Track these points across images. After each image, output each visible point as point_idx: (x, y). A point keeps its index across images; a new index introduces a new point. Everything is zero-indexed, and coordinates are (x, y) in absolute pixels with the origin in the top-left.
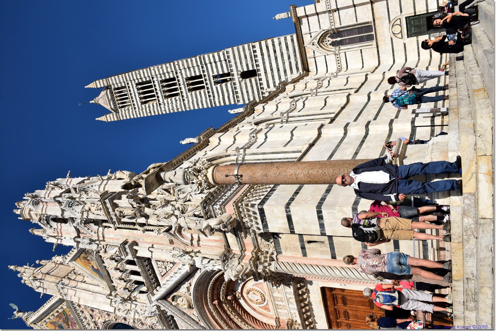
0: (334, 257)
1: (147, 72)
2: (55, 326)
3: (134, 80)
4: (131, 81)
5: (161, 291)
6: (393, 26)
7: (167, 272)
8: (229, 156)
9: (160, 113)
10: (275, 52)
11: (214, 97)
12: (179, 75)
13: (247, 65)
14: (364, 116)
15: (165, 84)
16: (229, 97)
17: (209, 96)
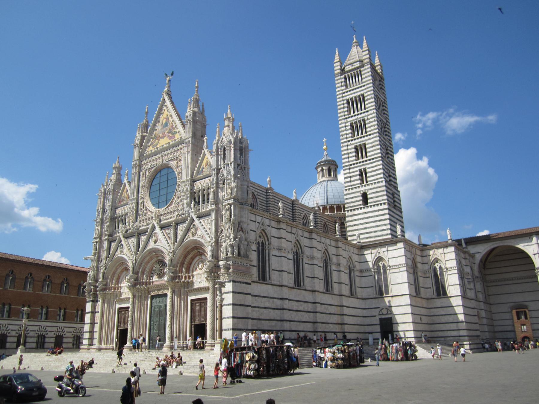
1: (372, 106)
2: (166, 119)
3: (366, 93)
4: (365, 89)
5: (196, 220)
6: (387, 309)
8: (268, 240)
9: (339, 119)
10: (380, 221)
11: (350, 169)
12: (368, 137)
13: (371, 198)
14: (297, 304)
15: (362, 123)
16: (351, 181)
17: (351, 165)
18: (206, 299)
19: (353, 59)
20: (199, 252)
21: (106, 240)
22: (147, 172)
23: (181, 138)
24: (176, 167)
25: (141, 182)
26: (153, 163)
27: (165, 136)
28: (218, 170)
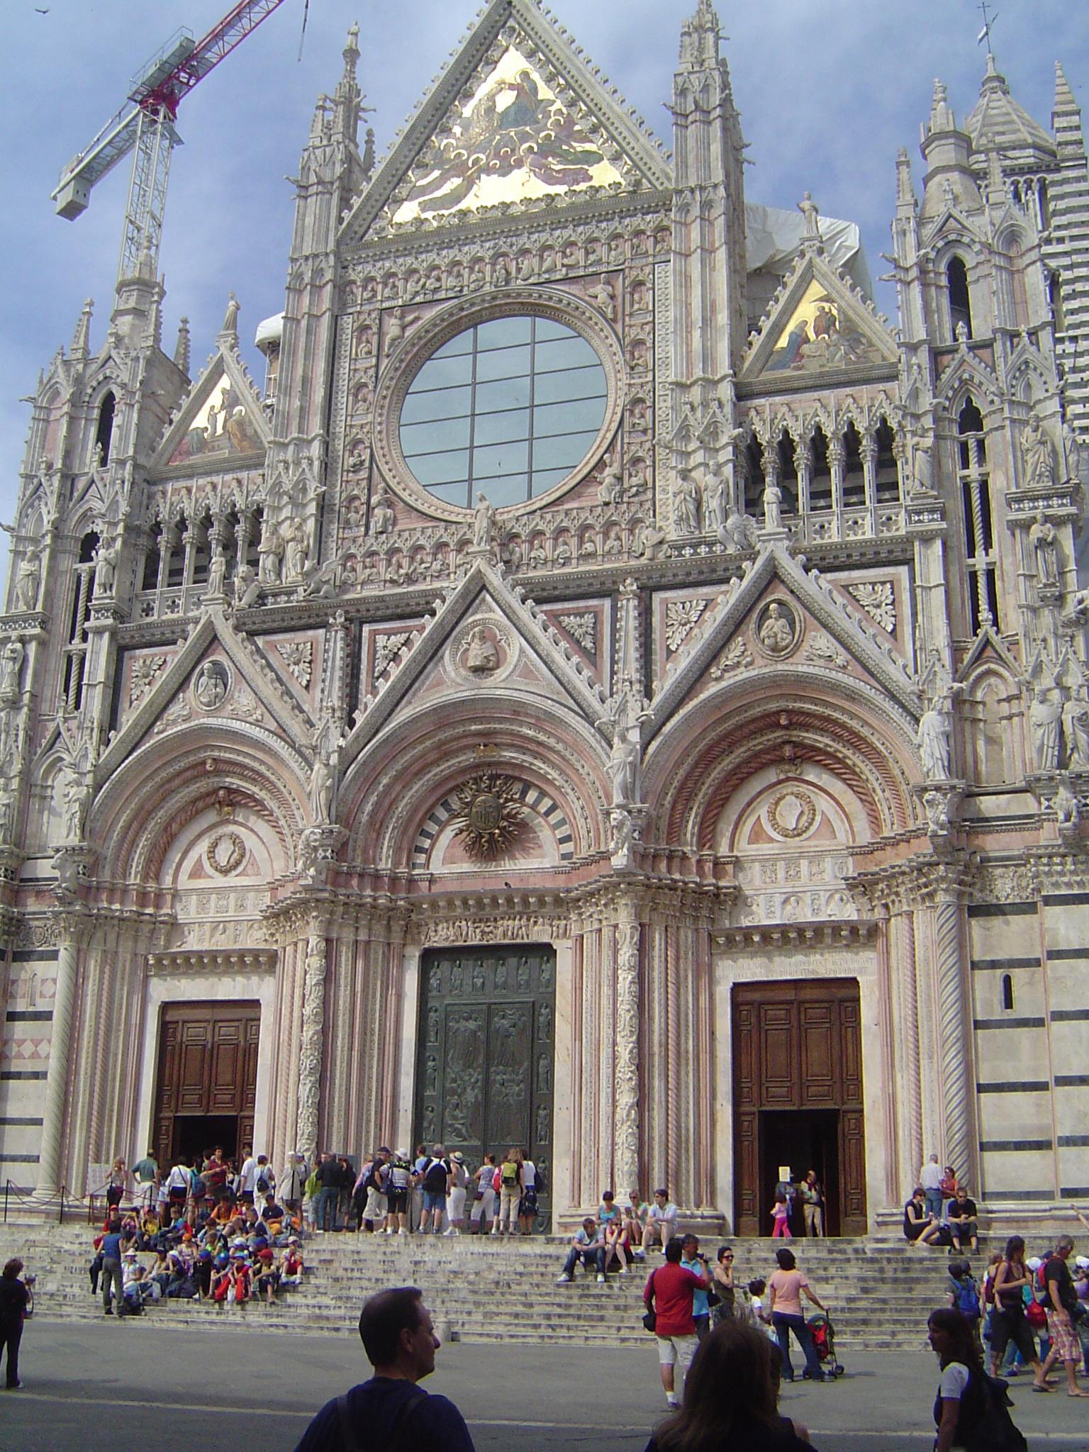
0: (978, 1025)
3: (1071, 267)
4: (1066, 254)
7: (863, 606)
18: (853, 982)
19: (1003, 133)
20: (796, 745)
21: (99, 632)
22: (392, 327)
23: (638, 183)
24: (610, 316)
25: (344, 368)
26: (431, 284)
27: (519, 164)
28: (936, 354)
